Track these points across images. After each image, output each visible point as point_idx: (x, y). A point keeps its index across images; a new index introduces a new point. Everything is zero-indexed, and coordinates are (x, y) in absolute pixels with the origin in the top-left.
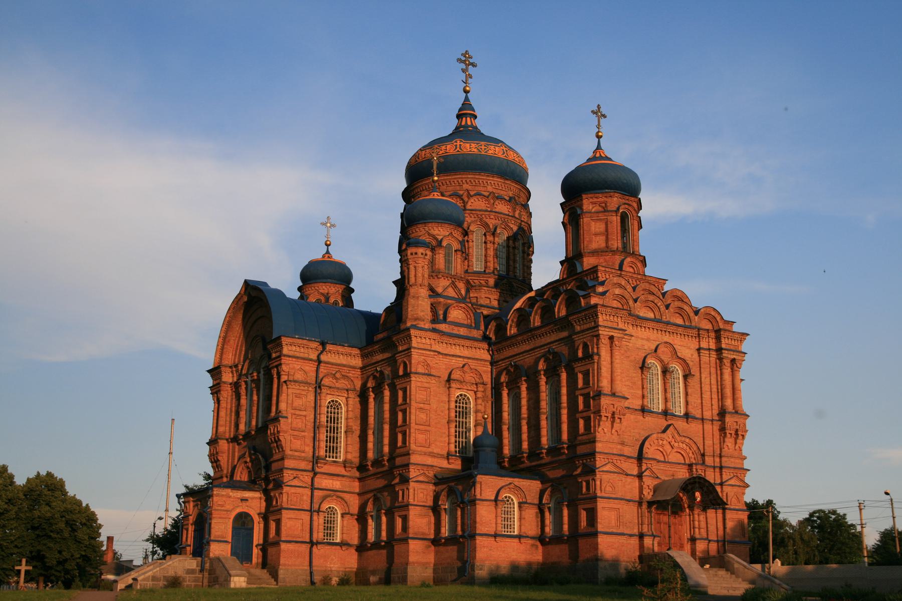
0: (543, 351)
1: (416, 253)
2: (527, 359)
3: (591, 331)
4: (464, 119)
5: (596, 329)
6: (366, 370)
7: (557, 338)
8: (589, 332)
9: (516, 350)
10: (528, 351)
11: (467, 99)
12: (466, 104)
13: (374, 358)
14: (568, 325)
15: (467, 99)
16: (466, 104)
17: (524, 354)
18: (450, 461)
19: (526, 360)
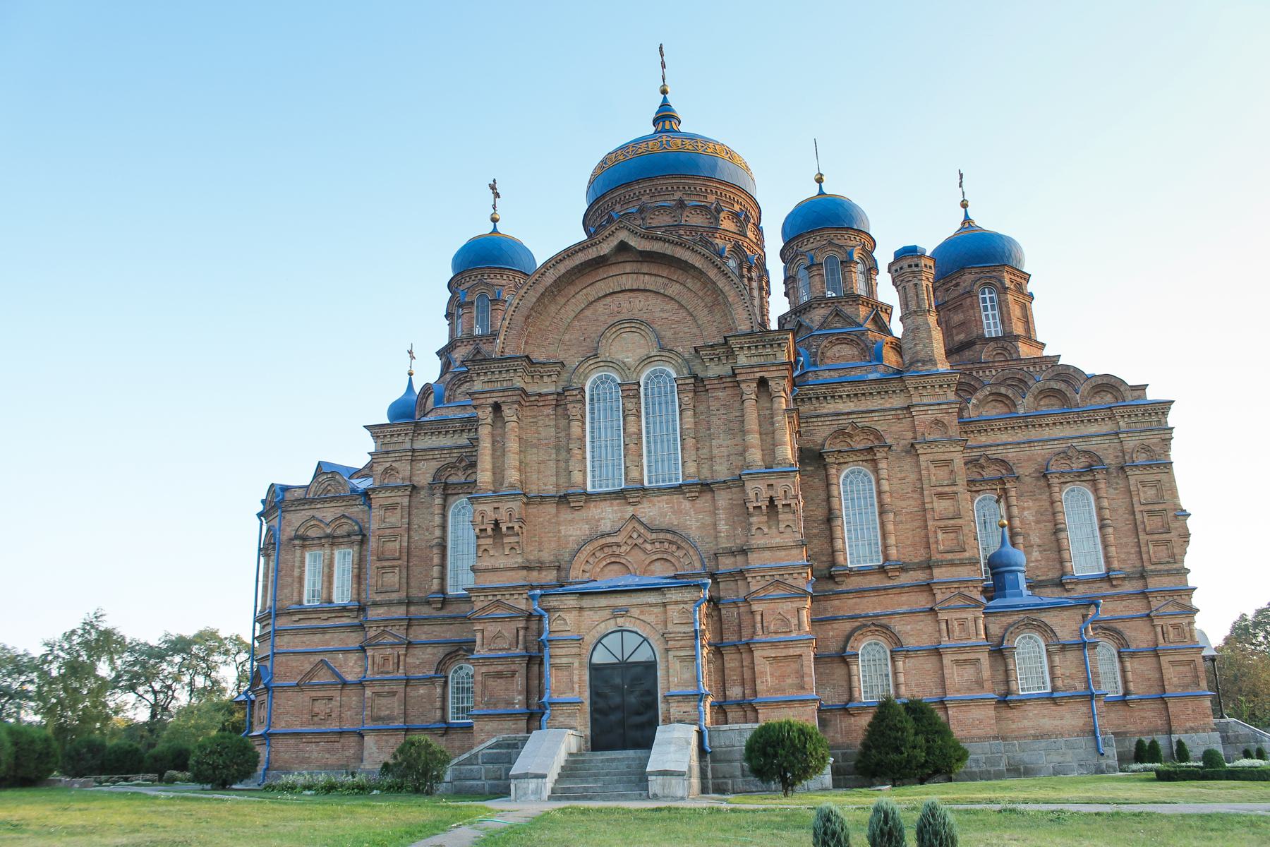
0: (1048, 447)
1: (917, 266)
2: (1014, 454)
3: (1156, 432)
4: (667, 122)
5: (1166, 431)
6: (807, 422)
7: (1078, 434)
8: (1152, 433)
9: (984, 439)
10: (1019, 443)
11: (665, 98)
12: (665, 105)
13: (829, 406)
14: (1103, 419)
15: (665, 98)
16: (665, 105)
17: (1009, 447)
18: (1114, 583)
19: (1010, 455)
